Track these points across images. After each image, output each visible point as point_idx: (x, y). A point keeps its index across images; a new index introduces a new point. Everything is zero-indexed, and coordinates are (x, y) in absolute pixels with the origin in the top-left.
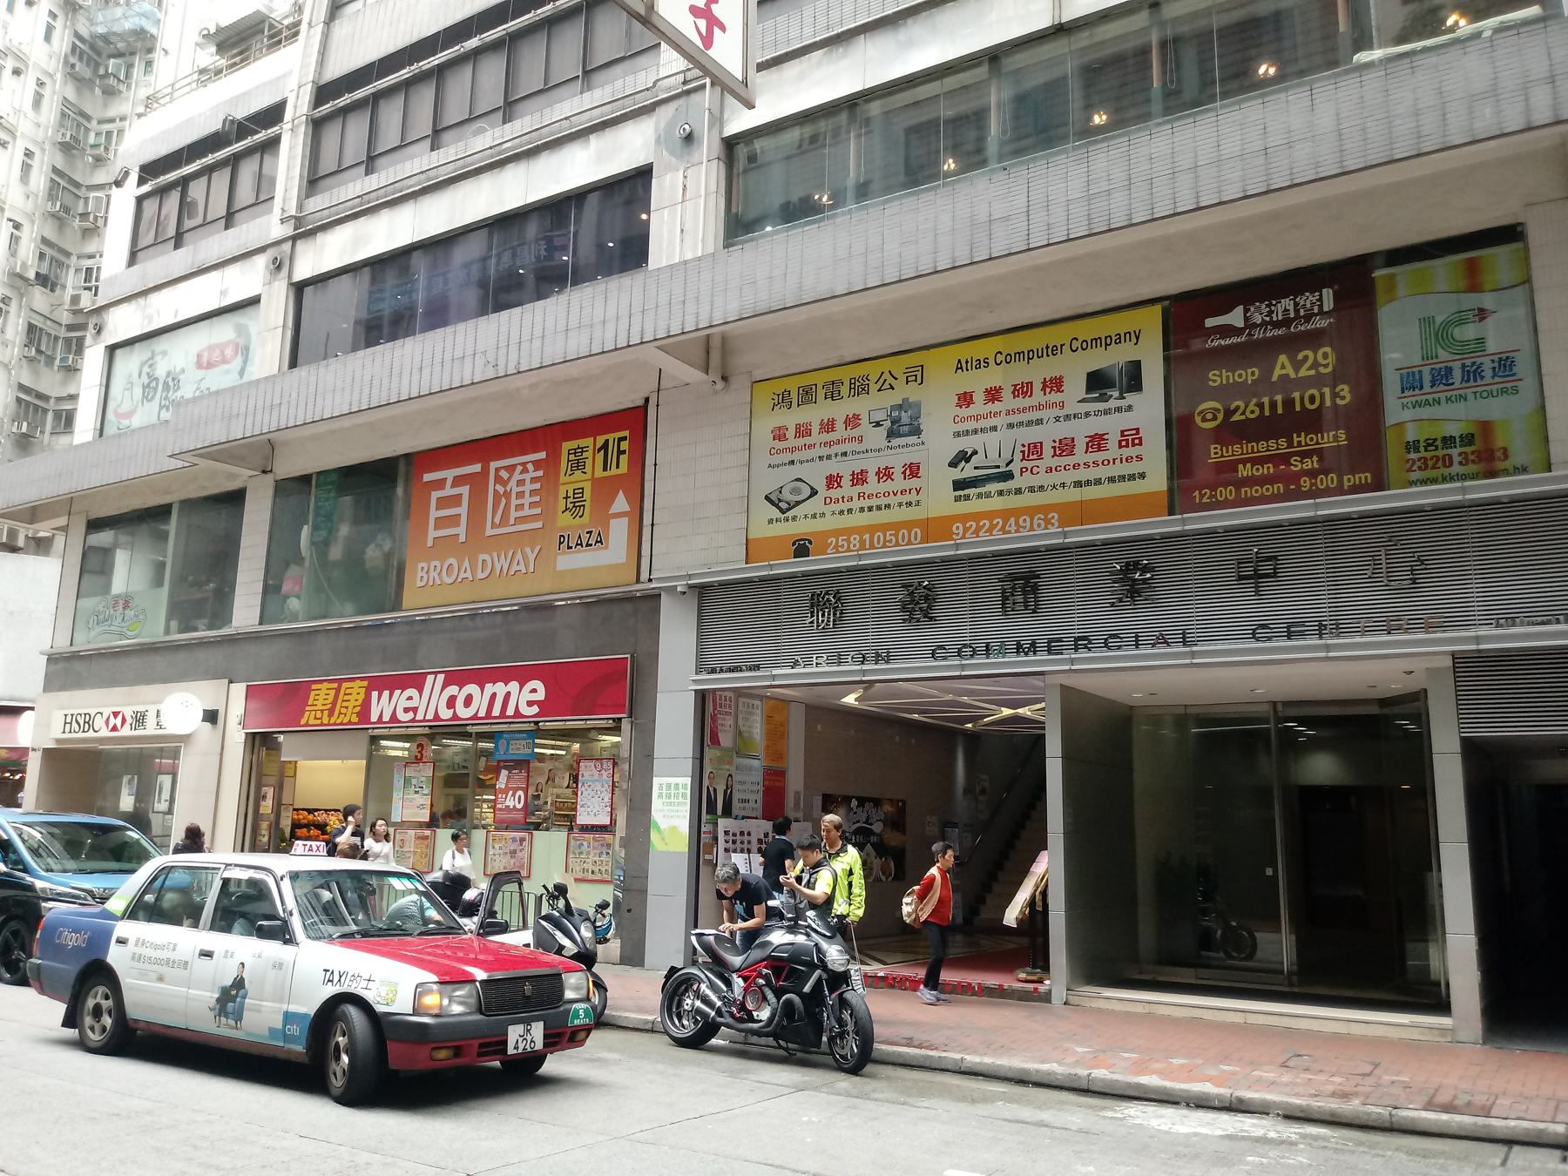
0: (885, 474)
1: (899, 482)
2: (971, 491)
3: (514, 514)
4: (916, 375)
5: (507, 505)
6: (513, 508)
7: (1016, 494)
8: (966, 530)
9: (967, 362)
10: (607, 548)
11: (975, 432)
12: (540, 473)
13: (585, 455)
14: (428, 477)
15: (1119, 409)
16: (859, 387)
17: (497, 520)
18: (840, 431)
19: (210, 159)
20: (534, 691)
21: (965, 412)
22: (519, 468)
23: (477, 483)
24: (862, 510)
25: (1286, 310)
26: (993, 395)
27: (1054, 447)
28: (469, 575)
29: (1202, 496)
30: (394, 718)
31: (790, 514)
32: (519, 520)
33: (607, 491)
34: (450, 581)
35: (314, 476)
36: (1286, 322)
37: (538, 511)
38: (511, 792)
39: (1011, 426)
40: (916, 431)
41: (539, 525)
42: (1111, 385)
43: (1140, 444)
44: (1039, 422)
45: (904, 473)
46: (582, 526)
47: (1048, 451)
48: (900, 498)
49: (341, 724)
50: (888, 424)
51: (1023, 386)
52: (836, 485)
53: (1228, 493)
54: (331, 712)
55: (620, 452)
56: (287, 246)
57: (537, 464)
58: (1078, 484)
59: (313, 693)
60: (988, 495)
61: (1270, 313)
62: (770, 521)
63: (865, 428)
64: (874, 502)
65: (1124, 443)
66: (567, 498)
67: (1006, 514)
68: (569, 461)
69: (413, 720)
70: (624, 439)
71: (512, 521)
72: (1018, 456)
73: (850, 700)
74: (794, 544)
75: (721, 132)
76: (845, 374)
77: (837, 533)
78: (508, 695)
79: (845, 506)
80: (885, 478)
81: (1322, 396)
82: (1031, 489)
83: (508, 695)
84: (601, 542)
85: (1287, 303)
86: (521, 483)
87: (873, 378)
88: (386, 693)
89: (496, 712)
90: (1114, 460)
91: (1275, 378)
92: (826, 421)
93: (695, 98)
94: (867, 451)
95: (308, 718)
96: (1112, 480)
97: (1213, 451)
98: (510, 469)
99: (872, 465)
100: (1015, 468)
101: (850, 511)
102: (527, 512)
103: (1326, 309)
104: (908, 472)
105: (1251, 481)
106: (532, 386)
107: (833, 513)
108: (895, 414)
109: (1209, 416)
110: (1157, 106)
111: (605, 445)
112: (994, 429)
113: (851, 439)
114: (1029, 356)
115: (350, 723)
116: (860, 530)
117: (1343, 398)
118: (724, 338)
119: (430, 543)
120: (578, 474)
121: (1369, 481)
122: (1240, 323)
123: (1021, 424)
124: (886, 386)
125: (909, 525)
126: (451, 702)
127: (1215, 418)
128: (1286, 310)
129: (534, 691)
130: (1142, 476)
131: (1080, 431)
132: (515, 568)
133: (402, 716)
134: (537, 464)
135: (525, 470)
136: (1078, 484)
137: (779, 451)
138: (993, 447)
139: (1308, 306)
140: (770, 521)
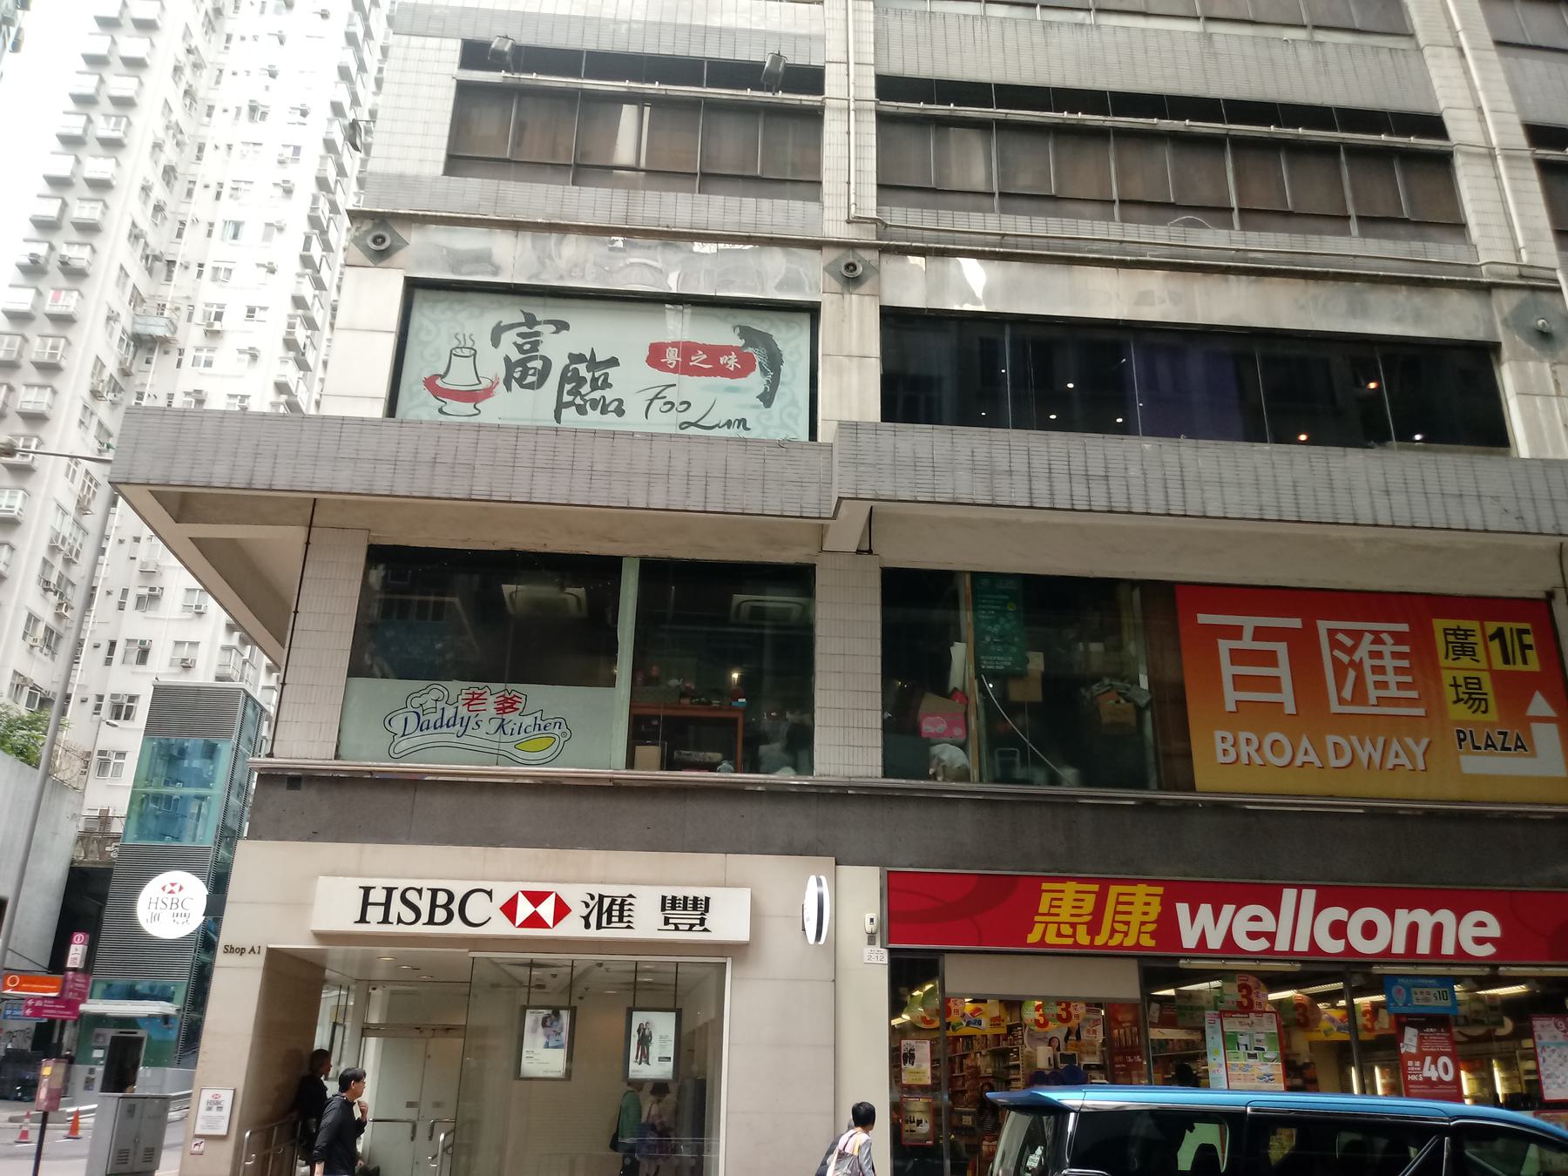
3: (1373, 694)
5: (1360, 680)
10: (1534, 755)
12: (1406, 649)
13: (1471, 639)
14: (1203, 619)
17: (1347, 693)
22: (1368, 637)
32: (1381, 701)
33: (1514, 690)
37: (1413, 694)
38: (1428, 1059)
41: (1420, 712)
46: (1491, 725)
49: (1120, 946)
54: (1094, 928)
57: (1398, 638)
59: (1045, 900)
68: (1447, 643)
69: (1270, 950)
70: (1526, 632)
71: (1373, 701)
78: (1438, 930)
83: (1438, 930)
88: (1205, 910)
89: (1424, 947)
98: (1357, 635)
102: (1393, 692)
106: (1367, 541)
111: (1500, 634)
115: (1138, 946)
119: (1230, 706)
120: (1465, 661)
129: (1481, 924)
132: (1391, 762)
135: (1382, 642)
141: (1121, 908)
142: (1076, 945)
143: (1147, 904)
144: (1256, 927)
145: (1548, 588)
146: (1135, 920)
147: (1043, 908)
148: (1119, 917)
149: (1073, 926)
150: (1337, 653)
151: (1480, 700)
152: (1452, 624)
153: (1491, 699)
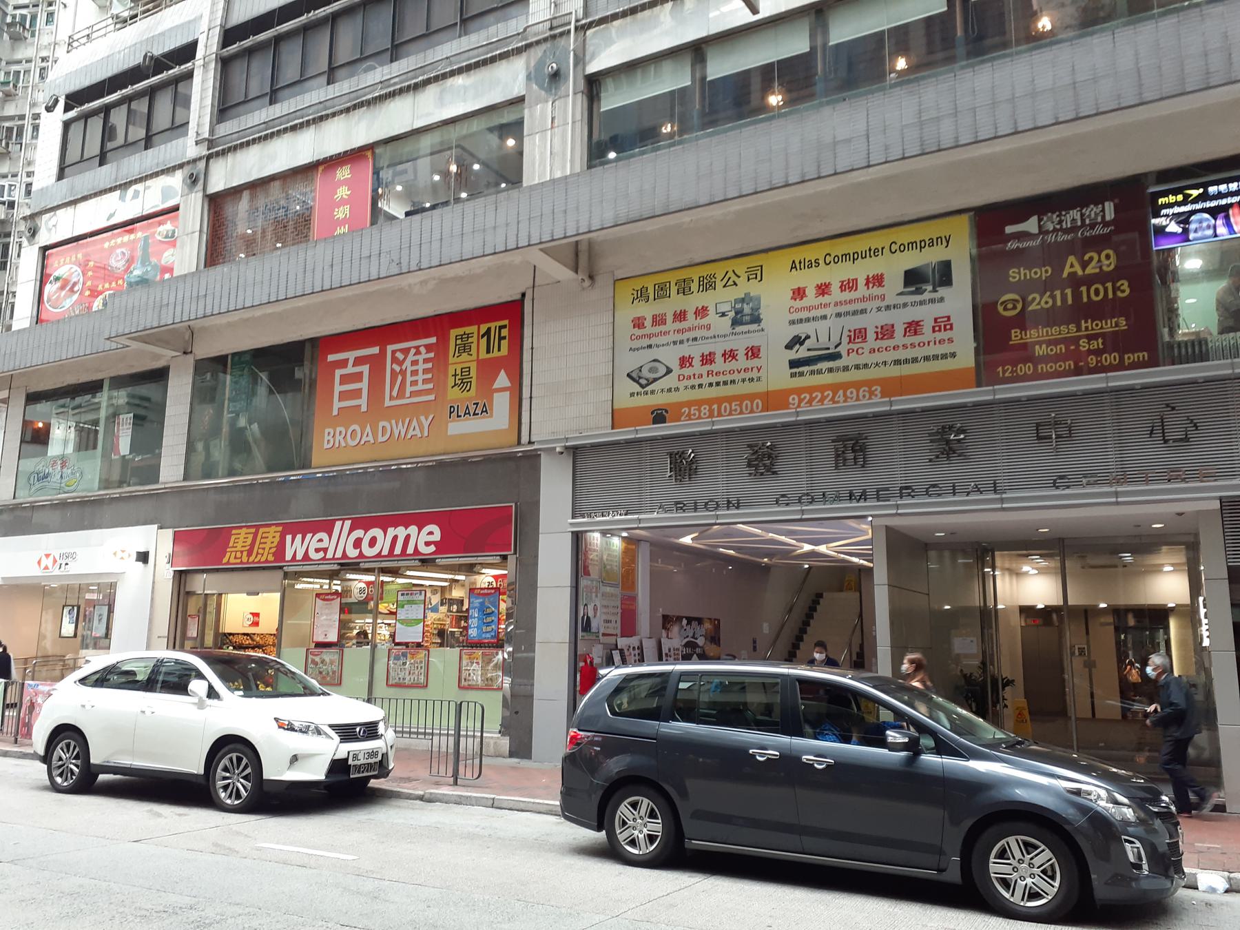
0: (730, 355)
1: (742, 362)
2: (805, 369)
3: (409, 389)
4: (756, 274)
6: (408, 383)
7: (844, 370)
8: (800, 401)
9: (800, 263)
11: (808, 320)
12: (432, 355)
13: (470, 340)
14: (331, 358)
15: (932, 301)
16: (707, 284)
17: (395, 393)
18: (691, 320)
19: (129, 90)
20: (431, 533)
21: (798, 304)
22: (413, 351)
23: (377, 363)
24: (711, 385)
25: (1073, 219)
26: (823, 289)
27: (877, 333)
28: (371, 438)
29: (1004, 372)
30: (306, 557)
31: (649, 388)
32: (413, 394)
33: (488, 369)
34: (355, 443)
35: (230, 357)
36: (1074, 229)
37: (430, 386)
39: (839, 315)
40: (756, 320)
41: (432, 397)
42: (924, 280)
43: (951, 329)
44: (863, 311)
45: (747, 354)
46: (470, 399)
47: (871, 335)
48: (743, 375)
49: (259, 562)
50: (732, 314)
51: (849, 283)
52: (688, 365)
53: (1027, 368)
54: (250, 553)
55: (501, 338)
56: (202, 165)
57: (429, 348)
58: (897, 362)
59: (233, 538)
60: (820, 372)
61: (1060, 222)
62: (632, 395)
63: (712, 318)
64: (721, 378)
65: (937, 329)
66: (455, 375)
67: (835, 388)
69: (324, 559)
70: (504, 327)
71: (408, 394)
72: (845, 340)
73: (687, 540)
74: (652, 413)
75: (584, 70)
76: (695, 274)
77: (689, 404)
78: (408, 538)
79: (696, 382)
80: (730, 359)
81: (1106, 290)
82: (857, 367)
83: (408, 538)
84: (486, 411)
85: (1075, 214)
86: (415, 363)
87: (720, 277)
88: (299, 537)
89: (398, 550)
90: (929, 342)
91: (1065, 275)
92: (678, 312)
93: (562, 42)
94: (715, 337)
95: (230, 558)
96: (927, 358)
97: (1013, 335)
98: (406, 351)
99: (719, 348)
100: (843, 349)
101: (700, 386)
102: (420, 387)
103: (1108, 218)
104: (750, 354)
105: (1046, 359)
106: (423, 283)
107: (686, 388)
108: (738, 306)
109: (1010, 306)
110: (961, 50)
111: (488, 331)
112: (825, 317)
113: (701, 327)
114: (854, 257)
115: (267, 561)
116: (709, 402)
117: (1123, 291)
118: (590, 243)
119: (335, 412)
120: (465, 356)
121: (1146, 358)
122: (1035, 230)
123: (847, 313)
124: (730, 282)
125: (752, 397)
126: (358, 543)
127: (1015, 308)
128: (1073, 219)
129: (431, 533)
130: (953, 355)
131: (899, 319)
132: (411, 433)
133: (313, 555)
134: (429, 348)
135: (418, 353)
136: (897, 362)
137: (639, 337)
138: (823, 333)
139: (1093, 215)
140: (632, 395)
141: (262, 541)
142: (242, 563)
143: (274, 537)
144: (320, 545)
145: (523, 291)
146: (267, 547)
147: (231, 544)
148: (261, 546)
149: (242, 552)
150: (395, 366)
151: (467, 382)
152: (460, 331)
153: (474, 381)
